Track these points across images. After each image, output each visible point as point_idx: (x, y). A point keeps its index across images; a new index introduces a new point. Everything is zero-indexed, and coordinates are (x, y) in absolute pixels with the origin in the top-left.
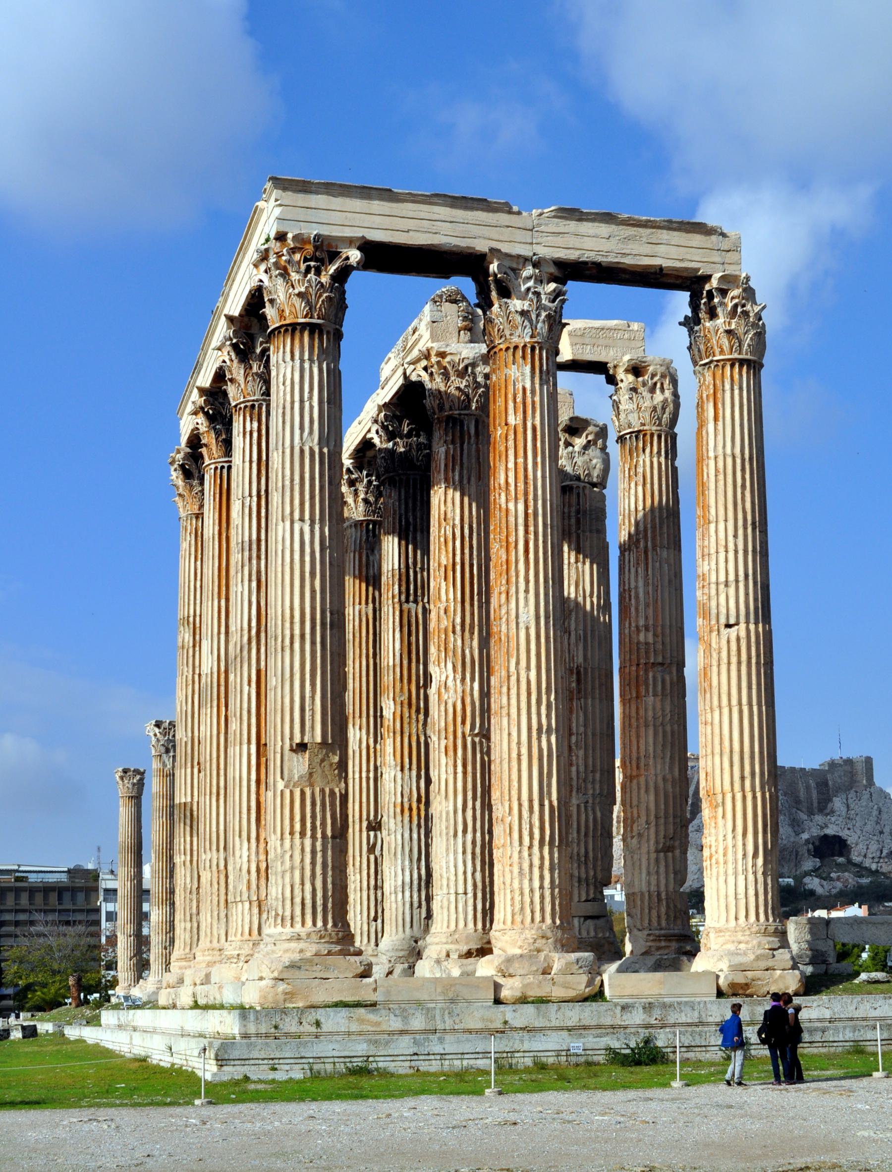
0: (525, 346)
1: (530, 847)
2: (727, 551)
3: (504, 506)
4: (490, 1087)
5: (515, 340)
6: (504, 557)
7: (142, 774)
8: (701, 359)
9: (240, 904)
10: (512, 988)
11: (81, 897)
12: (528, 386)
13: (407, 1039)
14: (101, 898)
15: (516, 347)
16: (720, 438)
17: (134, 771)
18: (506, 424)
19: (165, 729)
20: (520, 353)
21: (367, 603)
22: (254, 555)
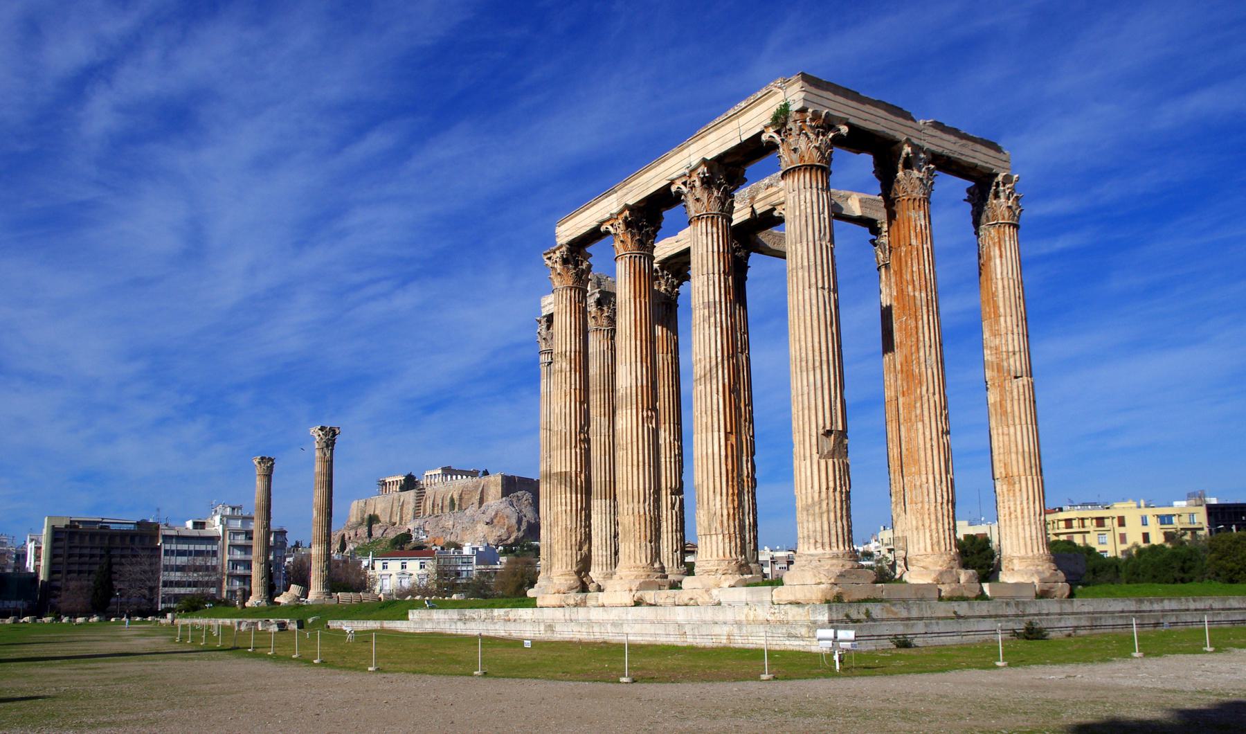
0: (920, 200)
1: (942, 504)
2: (1013, 334)
3: (912, 294)
4: (1135, 652)
5: (914, 195)
6: (913, 324)
7: (272, 460)
8: (988, 221)
9: (714, 537)
10: (946, 591)
11: (147, 540)
12: (923, 224)
13: (921, 623)
14: (161, 541)
15: (915, 199)
16: (1005, 267)
17: (269, 458)
18: (910, 245)
19: (326, 432)
20: (917, 203)
21: (667, 353)
22: (718, 310)
